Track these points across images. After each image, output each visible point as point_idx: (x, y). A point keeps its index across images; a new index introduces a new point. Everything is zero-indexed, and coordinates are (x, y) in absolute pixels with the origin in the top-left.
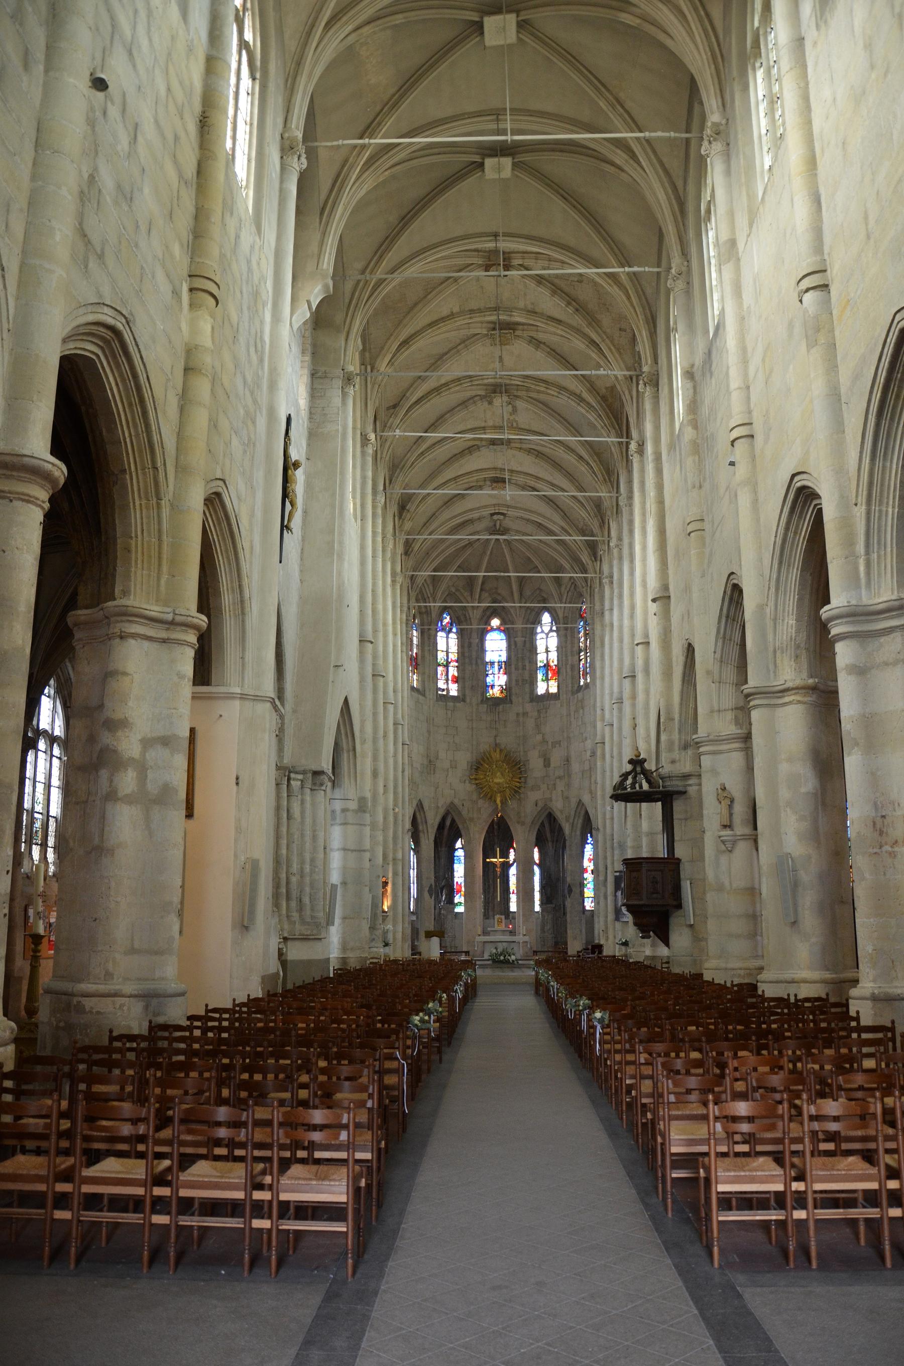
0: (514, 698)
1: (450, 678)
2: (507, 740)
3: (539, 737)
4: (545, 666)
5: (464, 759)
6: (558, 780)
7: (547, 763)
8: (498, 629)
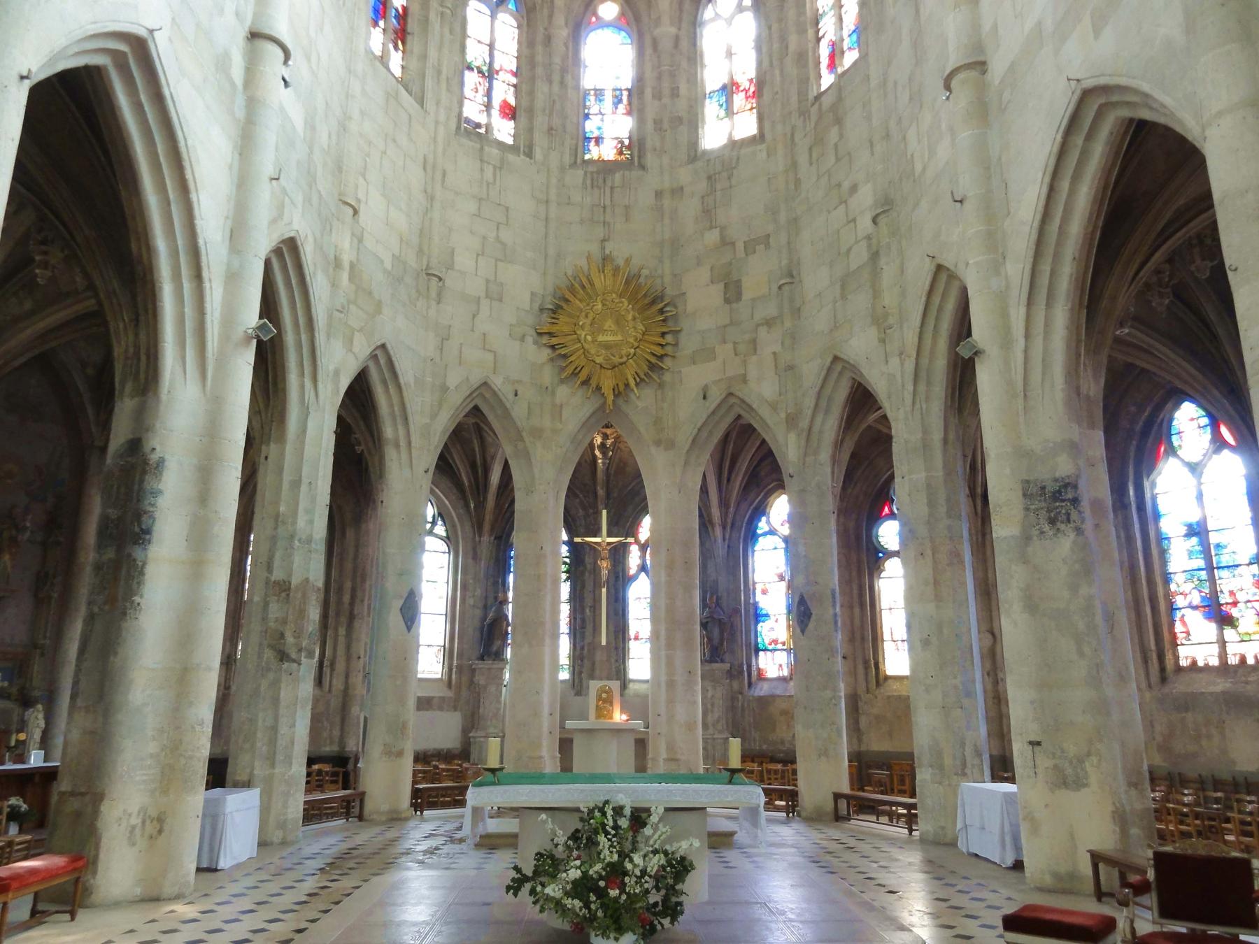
0: (650, 159)
1: (496, 103)
2: (633, 247)
3: (712, 237)
4: (724, 88)
5: (525, 286)
6: (763, 331)
7: (732, 292)
8: (615, 25)
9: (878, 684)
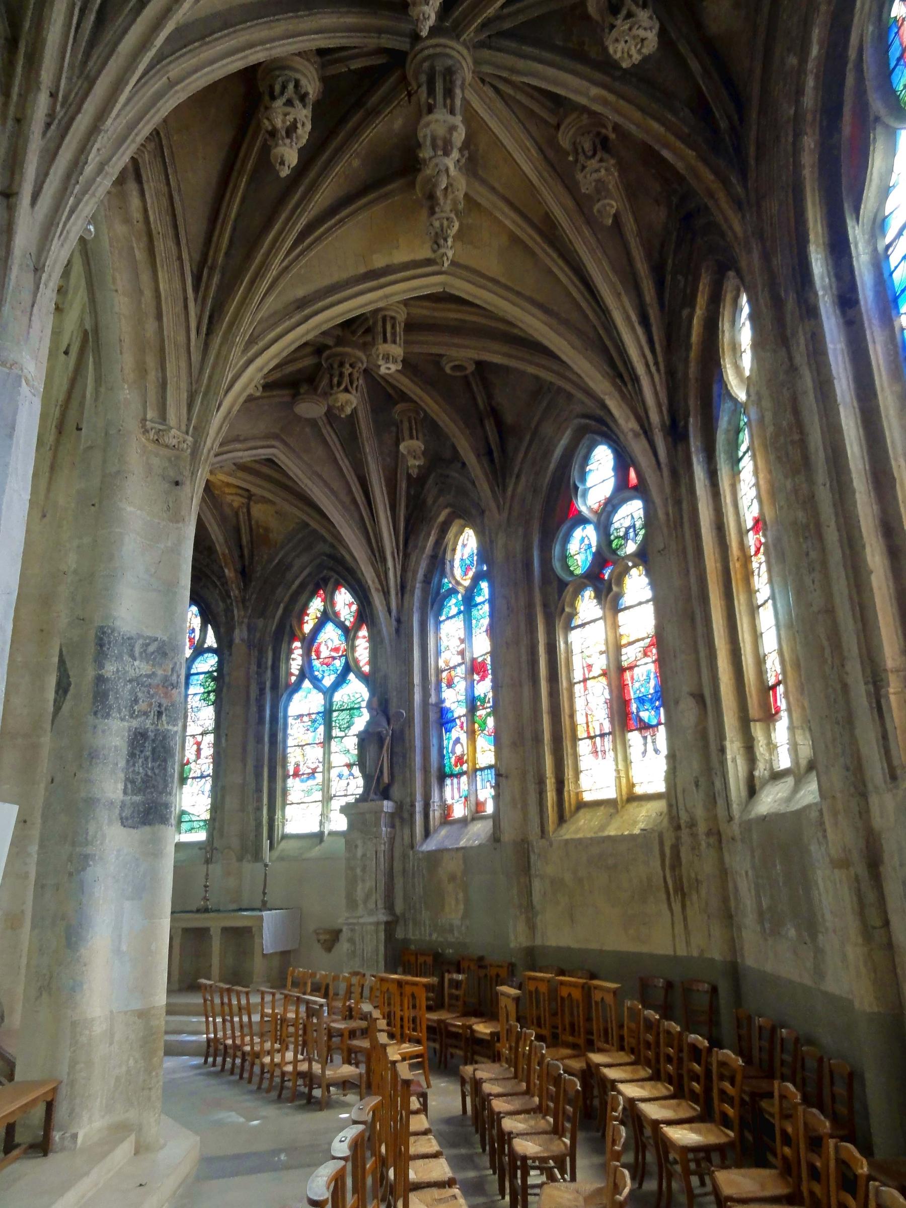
9: (561, 819)
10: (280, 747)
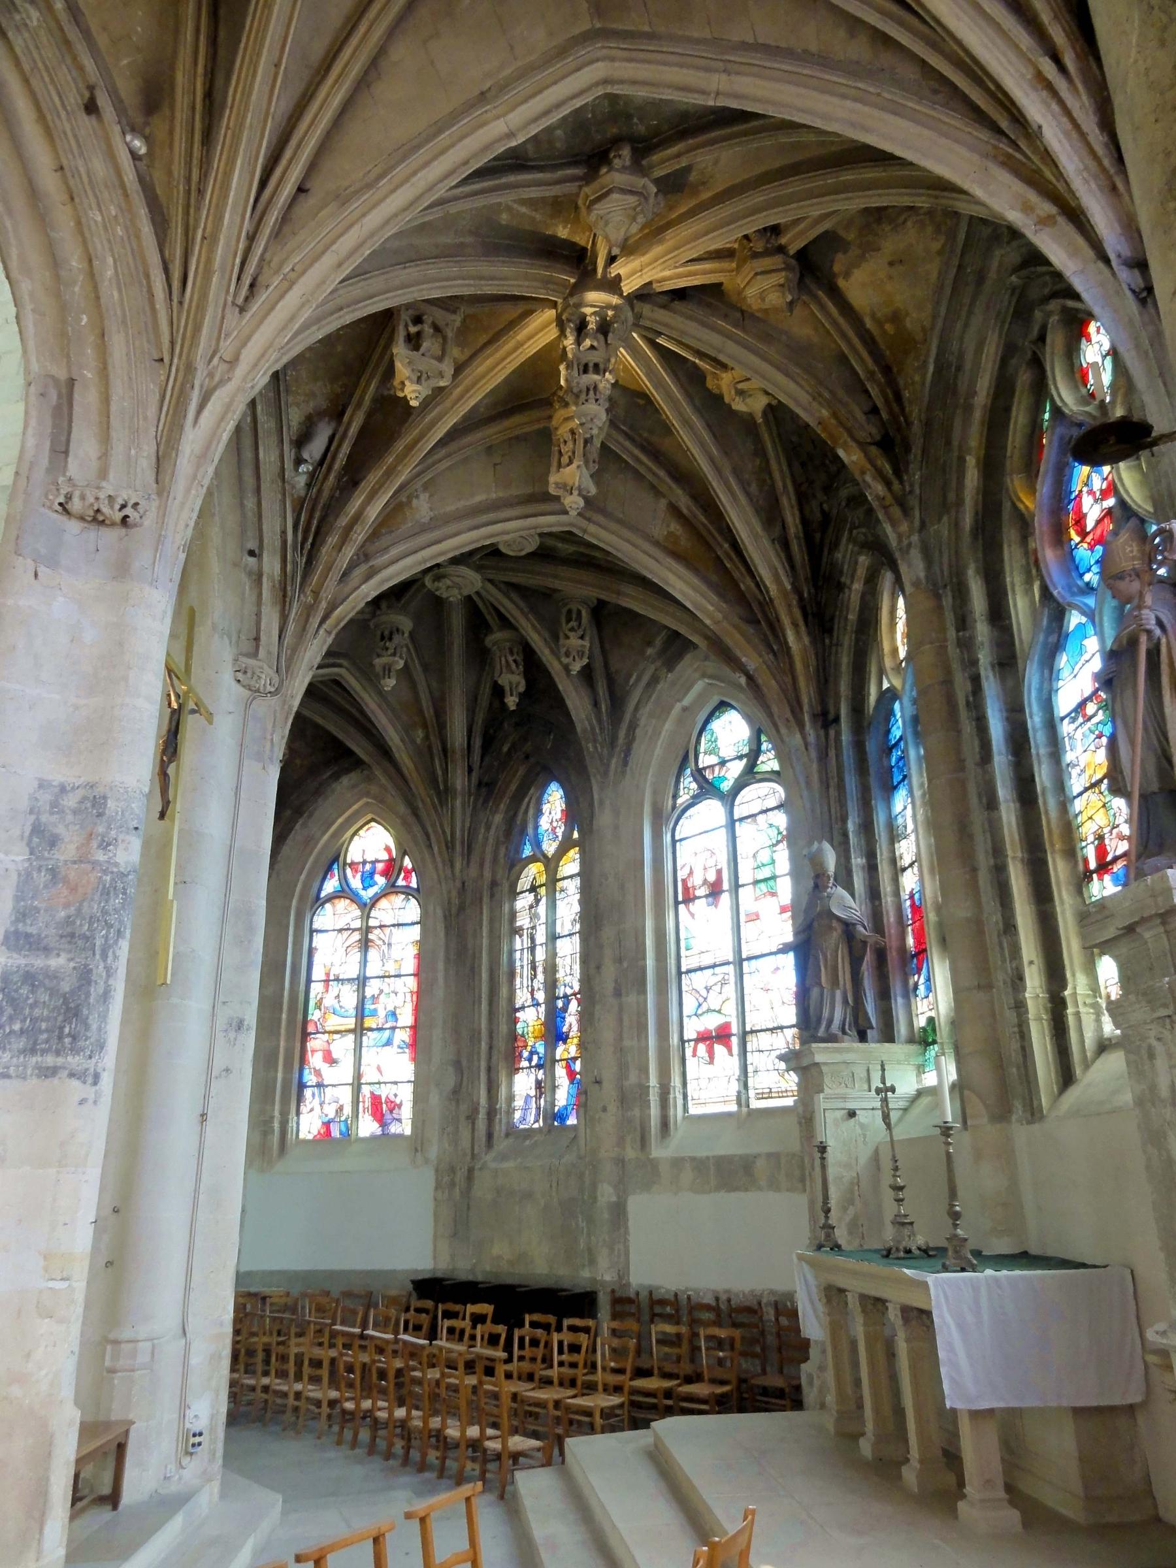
10: (1049, 805)
